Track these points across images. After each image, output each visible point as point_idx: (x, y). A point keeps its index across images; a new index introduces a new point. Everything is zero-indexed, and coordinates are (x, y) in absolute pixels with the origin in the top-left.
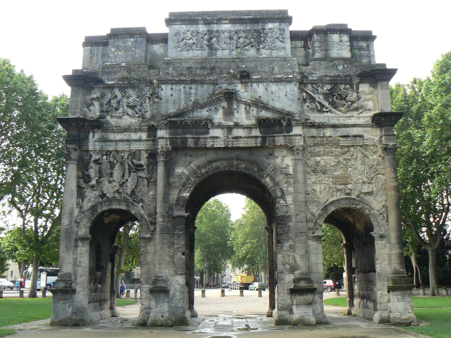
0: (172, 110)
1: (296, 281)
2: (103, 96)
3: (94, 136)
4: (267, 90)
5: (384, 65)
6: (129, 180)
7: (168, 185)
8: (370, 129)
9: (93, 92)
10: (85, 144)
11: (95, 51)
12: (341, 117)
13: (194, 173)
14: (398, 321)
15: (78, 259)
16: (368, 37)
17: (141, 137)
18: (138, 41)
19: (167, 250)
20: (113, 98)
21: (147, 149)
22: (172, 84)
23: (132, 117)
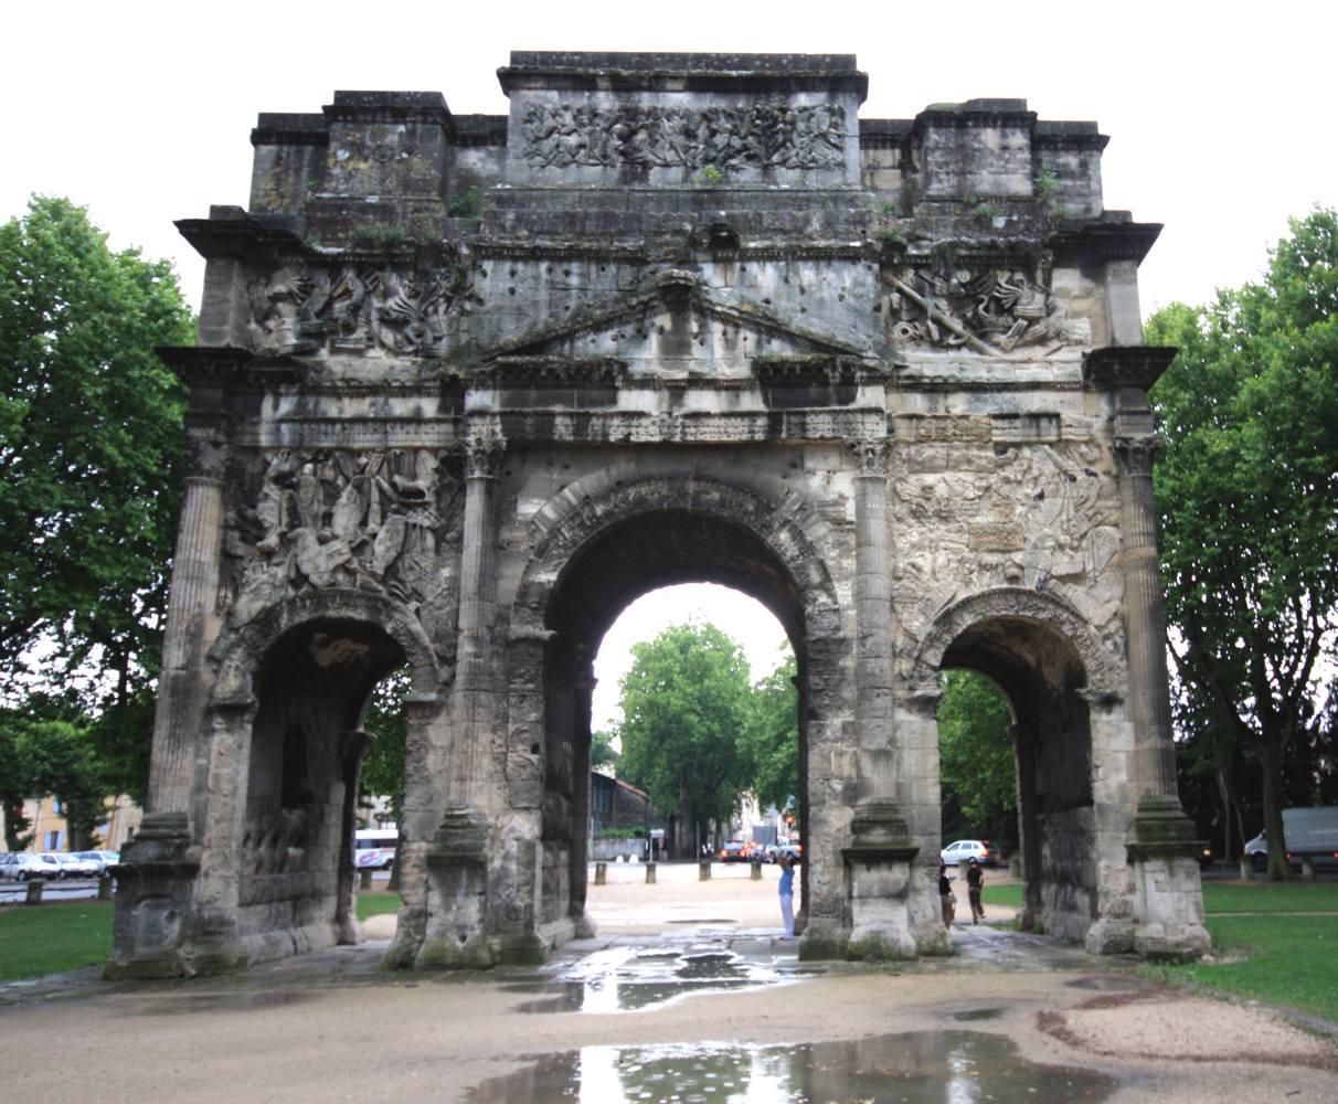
0: (512, 333)
1: (858, 826)
2: (307, 289)
3: (276, 407)
4: (786, 281)
5: (1127, 214)
6: (382, 535)
7: (496, 549)
8: (1078, 396)
9: (277, 276)
10: (248, 429)
11: (292, 158)
12: (998, 362)
13: (572, 514)
14: (1159, 948)
16: (1086, 139)
17: (418, 410)
18: (419, 132)
19: (485, 737)
20: (340, 296)
21: (436, 444)
22: (515, 259)
23: (396, 351)
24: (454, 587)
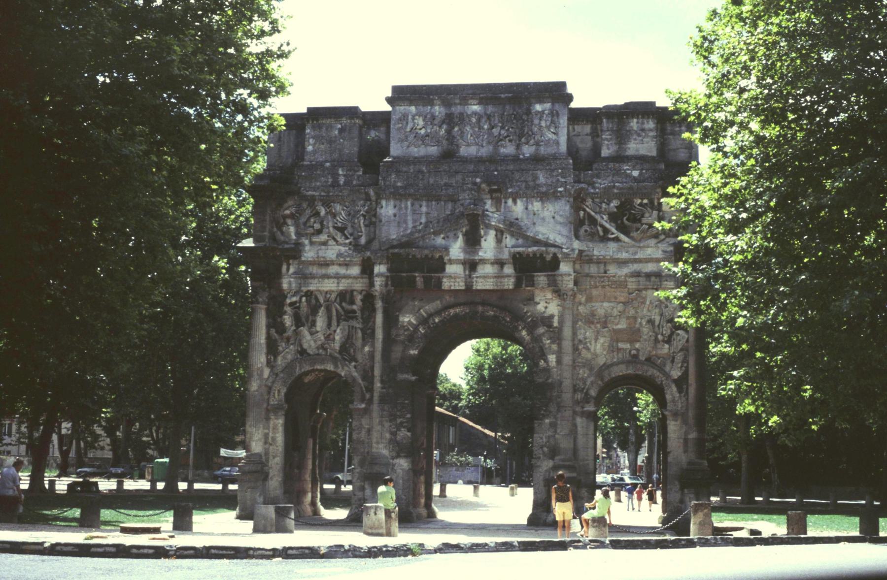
3: (288, 270)
4: (527, 209)
6: (338, 331)
7: (389, 341)
13: (424, 321)
15: (271, 434)
19: (387, 425)
24: (372, 355)
